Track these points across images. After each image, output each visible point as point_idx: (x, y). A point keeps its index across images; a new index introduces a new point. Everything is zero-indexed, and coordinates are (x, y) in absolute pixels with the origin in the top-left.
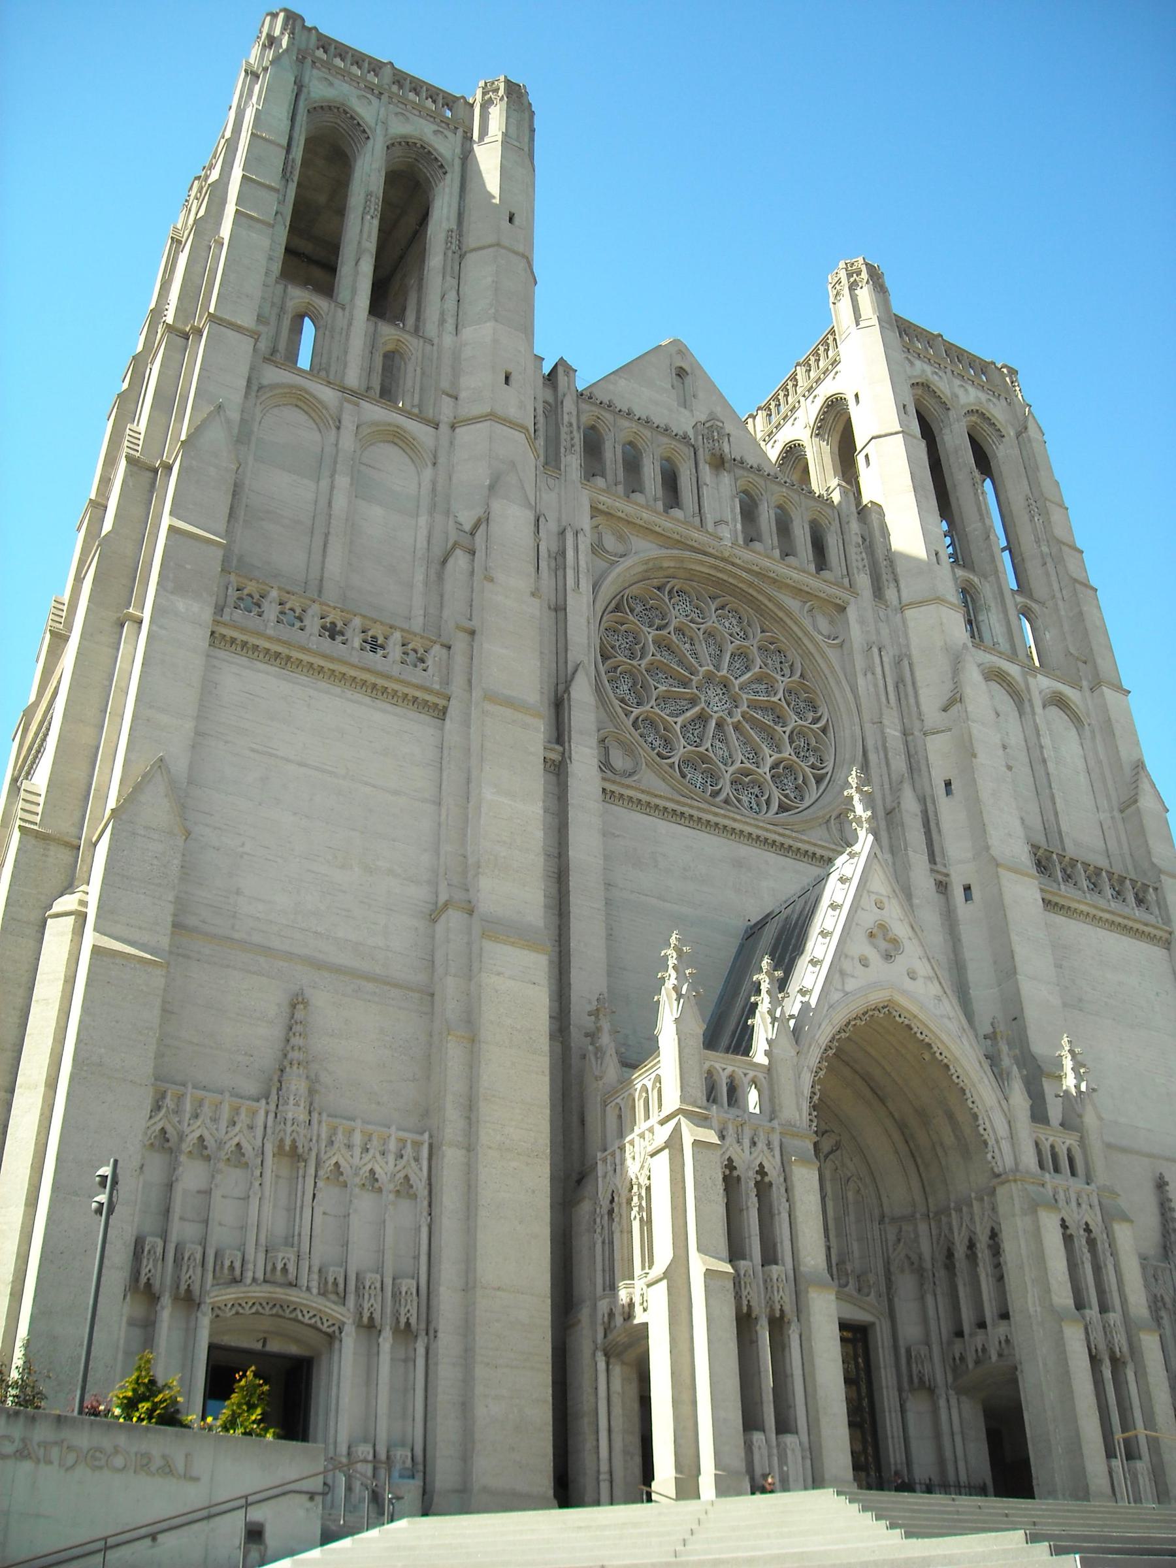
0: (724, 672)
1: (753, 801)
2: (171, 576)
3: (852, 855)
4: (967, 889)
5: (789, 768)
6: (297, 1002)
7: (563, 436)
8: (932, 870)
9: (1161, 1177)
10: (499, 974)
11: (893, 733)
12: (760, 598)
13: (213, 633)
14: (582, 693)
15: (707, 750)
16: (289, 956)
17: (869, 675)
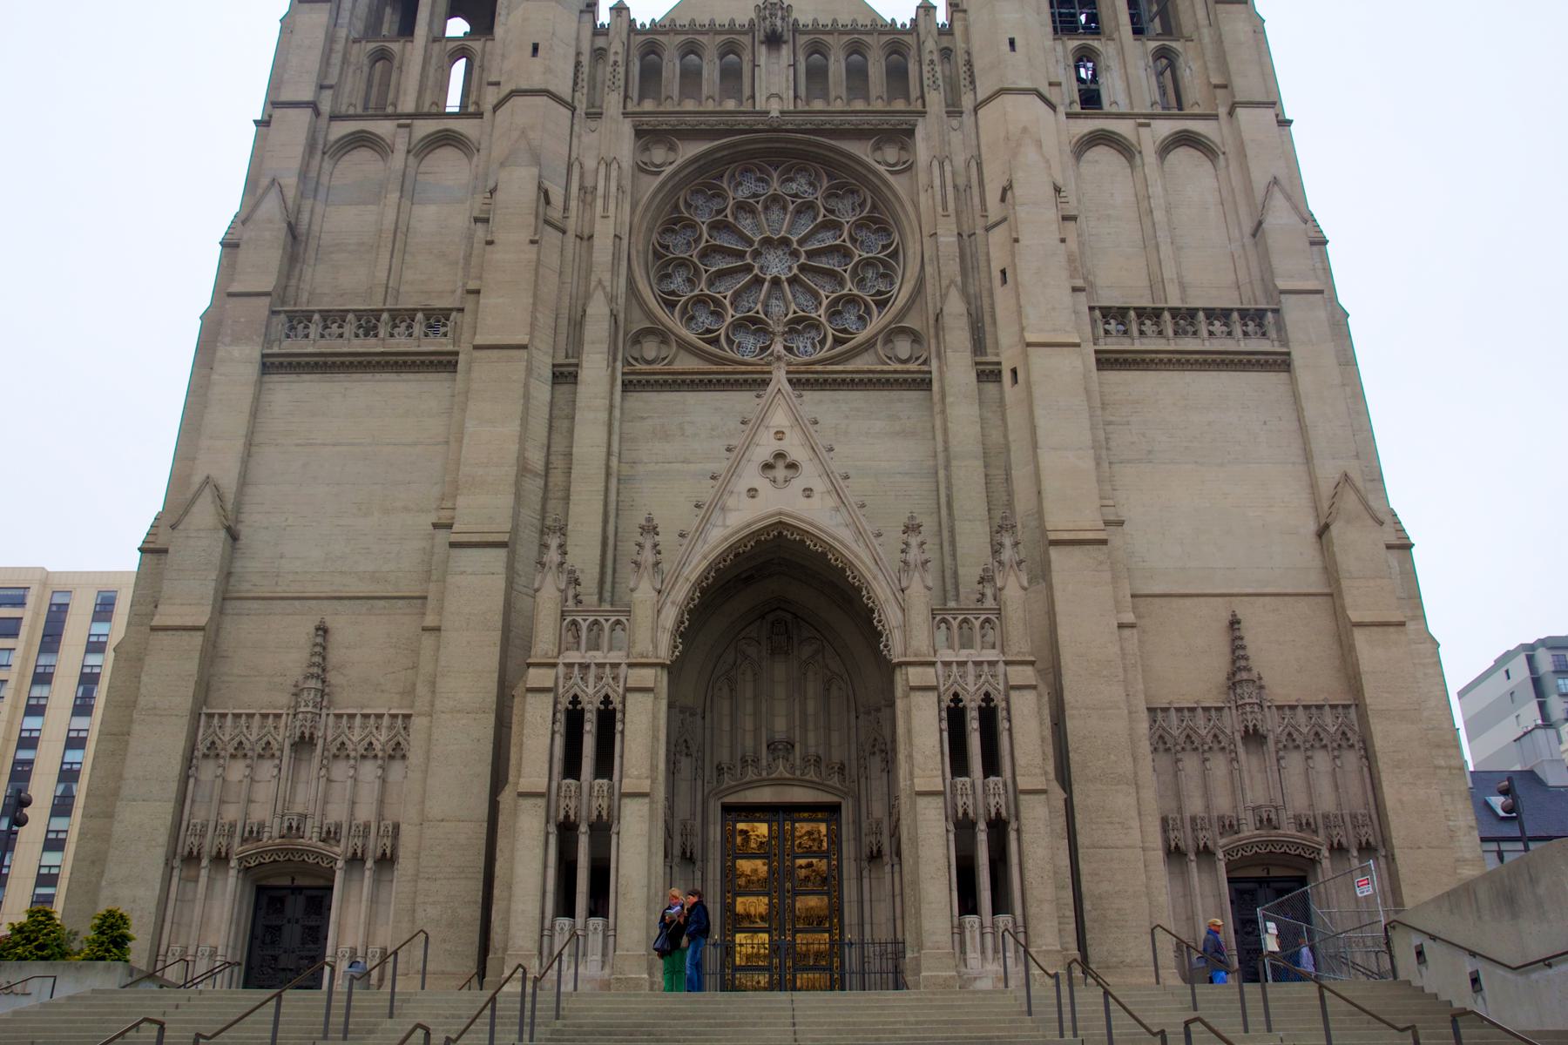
0: (782, 233)
1: (809, 345)
2: (229, 332)
3: (758, 396)
4: (1014, 372)
5: (852, 300)
8: (977, 364)
9: (1234, 615)
10: (462, 573)
11: (948, 239)
12: (821, 151)
13: (264, 364)
14: (598, 310)
15: (850, 290)
17: (930, 190)
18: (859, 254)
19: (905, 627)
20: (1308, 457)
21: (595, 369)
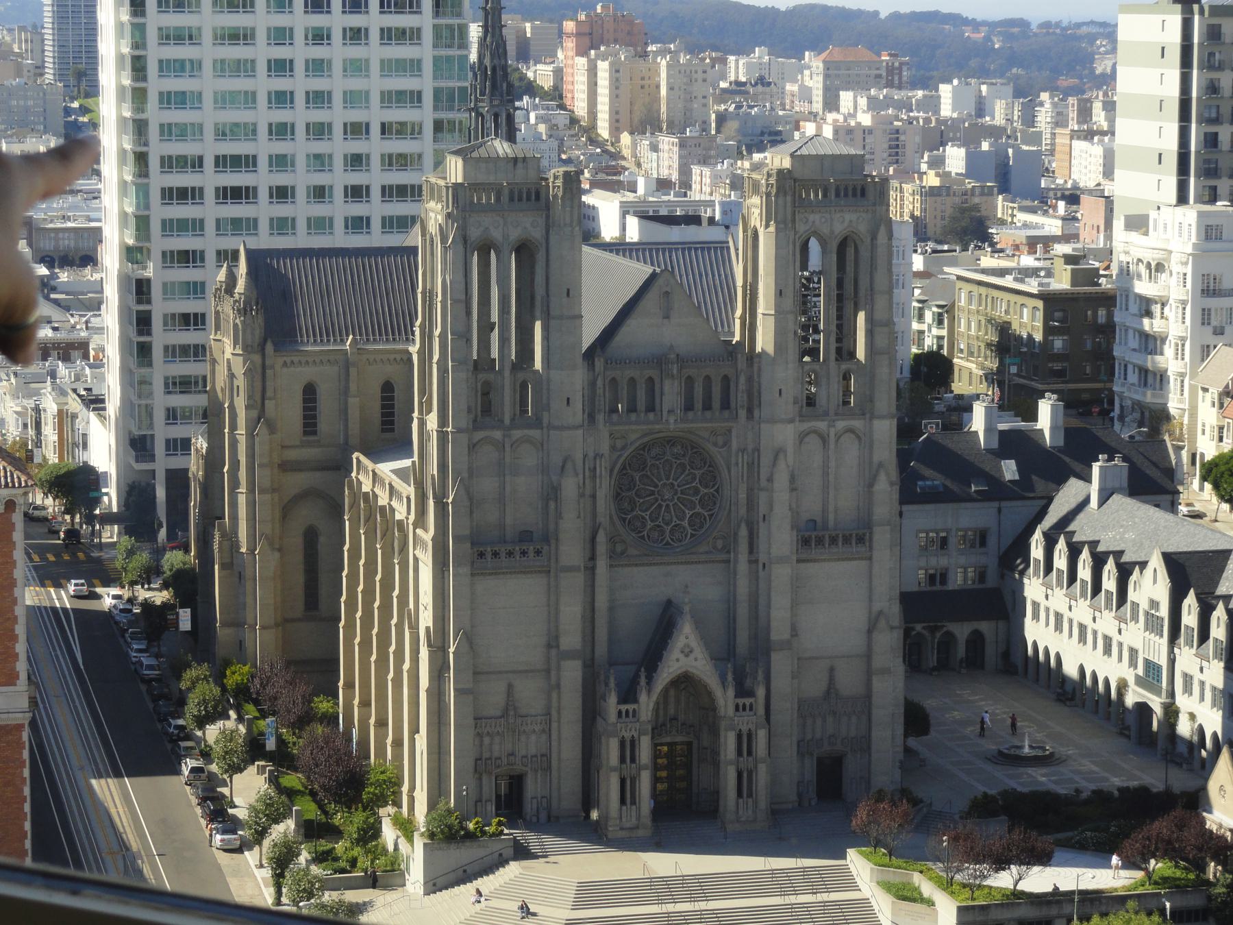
4: (764, 564)
6: (510, 687)
7: (597, 403)
11: (743, 496)
14: (601, 538)
16: (507, 672)
18: (704, 491)
19: (726, 705)
20: (870, 600)
21: (602, 565)
